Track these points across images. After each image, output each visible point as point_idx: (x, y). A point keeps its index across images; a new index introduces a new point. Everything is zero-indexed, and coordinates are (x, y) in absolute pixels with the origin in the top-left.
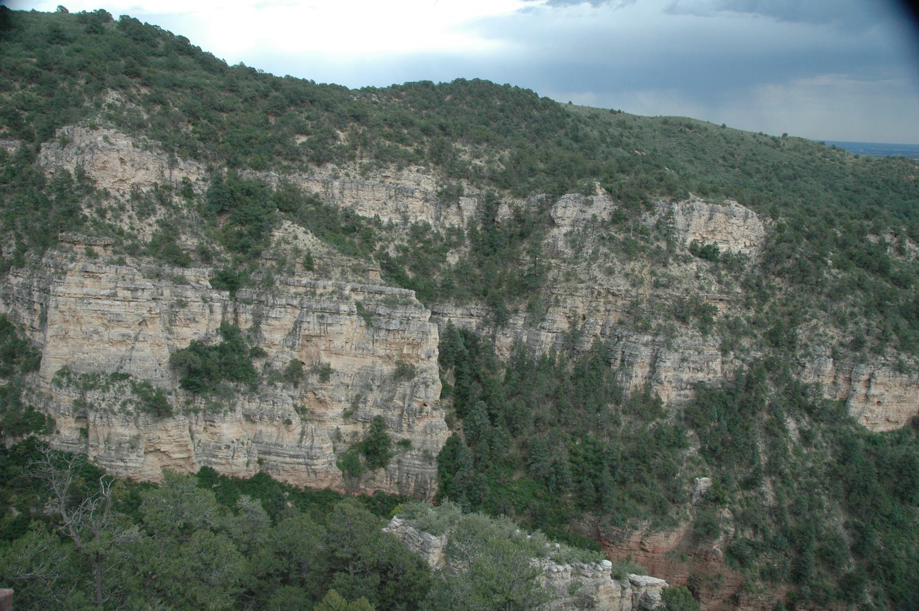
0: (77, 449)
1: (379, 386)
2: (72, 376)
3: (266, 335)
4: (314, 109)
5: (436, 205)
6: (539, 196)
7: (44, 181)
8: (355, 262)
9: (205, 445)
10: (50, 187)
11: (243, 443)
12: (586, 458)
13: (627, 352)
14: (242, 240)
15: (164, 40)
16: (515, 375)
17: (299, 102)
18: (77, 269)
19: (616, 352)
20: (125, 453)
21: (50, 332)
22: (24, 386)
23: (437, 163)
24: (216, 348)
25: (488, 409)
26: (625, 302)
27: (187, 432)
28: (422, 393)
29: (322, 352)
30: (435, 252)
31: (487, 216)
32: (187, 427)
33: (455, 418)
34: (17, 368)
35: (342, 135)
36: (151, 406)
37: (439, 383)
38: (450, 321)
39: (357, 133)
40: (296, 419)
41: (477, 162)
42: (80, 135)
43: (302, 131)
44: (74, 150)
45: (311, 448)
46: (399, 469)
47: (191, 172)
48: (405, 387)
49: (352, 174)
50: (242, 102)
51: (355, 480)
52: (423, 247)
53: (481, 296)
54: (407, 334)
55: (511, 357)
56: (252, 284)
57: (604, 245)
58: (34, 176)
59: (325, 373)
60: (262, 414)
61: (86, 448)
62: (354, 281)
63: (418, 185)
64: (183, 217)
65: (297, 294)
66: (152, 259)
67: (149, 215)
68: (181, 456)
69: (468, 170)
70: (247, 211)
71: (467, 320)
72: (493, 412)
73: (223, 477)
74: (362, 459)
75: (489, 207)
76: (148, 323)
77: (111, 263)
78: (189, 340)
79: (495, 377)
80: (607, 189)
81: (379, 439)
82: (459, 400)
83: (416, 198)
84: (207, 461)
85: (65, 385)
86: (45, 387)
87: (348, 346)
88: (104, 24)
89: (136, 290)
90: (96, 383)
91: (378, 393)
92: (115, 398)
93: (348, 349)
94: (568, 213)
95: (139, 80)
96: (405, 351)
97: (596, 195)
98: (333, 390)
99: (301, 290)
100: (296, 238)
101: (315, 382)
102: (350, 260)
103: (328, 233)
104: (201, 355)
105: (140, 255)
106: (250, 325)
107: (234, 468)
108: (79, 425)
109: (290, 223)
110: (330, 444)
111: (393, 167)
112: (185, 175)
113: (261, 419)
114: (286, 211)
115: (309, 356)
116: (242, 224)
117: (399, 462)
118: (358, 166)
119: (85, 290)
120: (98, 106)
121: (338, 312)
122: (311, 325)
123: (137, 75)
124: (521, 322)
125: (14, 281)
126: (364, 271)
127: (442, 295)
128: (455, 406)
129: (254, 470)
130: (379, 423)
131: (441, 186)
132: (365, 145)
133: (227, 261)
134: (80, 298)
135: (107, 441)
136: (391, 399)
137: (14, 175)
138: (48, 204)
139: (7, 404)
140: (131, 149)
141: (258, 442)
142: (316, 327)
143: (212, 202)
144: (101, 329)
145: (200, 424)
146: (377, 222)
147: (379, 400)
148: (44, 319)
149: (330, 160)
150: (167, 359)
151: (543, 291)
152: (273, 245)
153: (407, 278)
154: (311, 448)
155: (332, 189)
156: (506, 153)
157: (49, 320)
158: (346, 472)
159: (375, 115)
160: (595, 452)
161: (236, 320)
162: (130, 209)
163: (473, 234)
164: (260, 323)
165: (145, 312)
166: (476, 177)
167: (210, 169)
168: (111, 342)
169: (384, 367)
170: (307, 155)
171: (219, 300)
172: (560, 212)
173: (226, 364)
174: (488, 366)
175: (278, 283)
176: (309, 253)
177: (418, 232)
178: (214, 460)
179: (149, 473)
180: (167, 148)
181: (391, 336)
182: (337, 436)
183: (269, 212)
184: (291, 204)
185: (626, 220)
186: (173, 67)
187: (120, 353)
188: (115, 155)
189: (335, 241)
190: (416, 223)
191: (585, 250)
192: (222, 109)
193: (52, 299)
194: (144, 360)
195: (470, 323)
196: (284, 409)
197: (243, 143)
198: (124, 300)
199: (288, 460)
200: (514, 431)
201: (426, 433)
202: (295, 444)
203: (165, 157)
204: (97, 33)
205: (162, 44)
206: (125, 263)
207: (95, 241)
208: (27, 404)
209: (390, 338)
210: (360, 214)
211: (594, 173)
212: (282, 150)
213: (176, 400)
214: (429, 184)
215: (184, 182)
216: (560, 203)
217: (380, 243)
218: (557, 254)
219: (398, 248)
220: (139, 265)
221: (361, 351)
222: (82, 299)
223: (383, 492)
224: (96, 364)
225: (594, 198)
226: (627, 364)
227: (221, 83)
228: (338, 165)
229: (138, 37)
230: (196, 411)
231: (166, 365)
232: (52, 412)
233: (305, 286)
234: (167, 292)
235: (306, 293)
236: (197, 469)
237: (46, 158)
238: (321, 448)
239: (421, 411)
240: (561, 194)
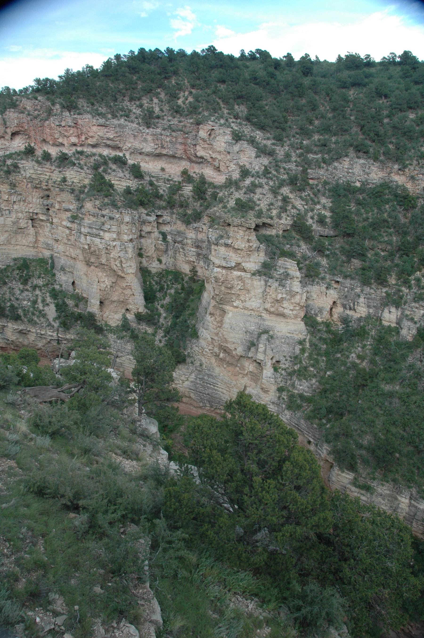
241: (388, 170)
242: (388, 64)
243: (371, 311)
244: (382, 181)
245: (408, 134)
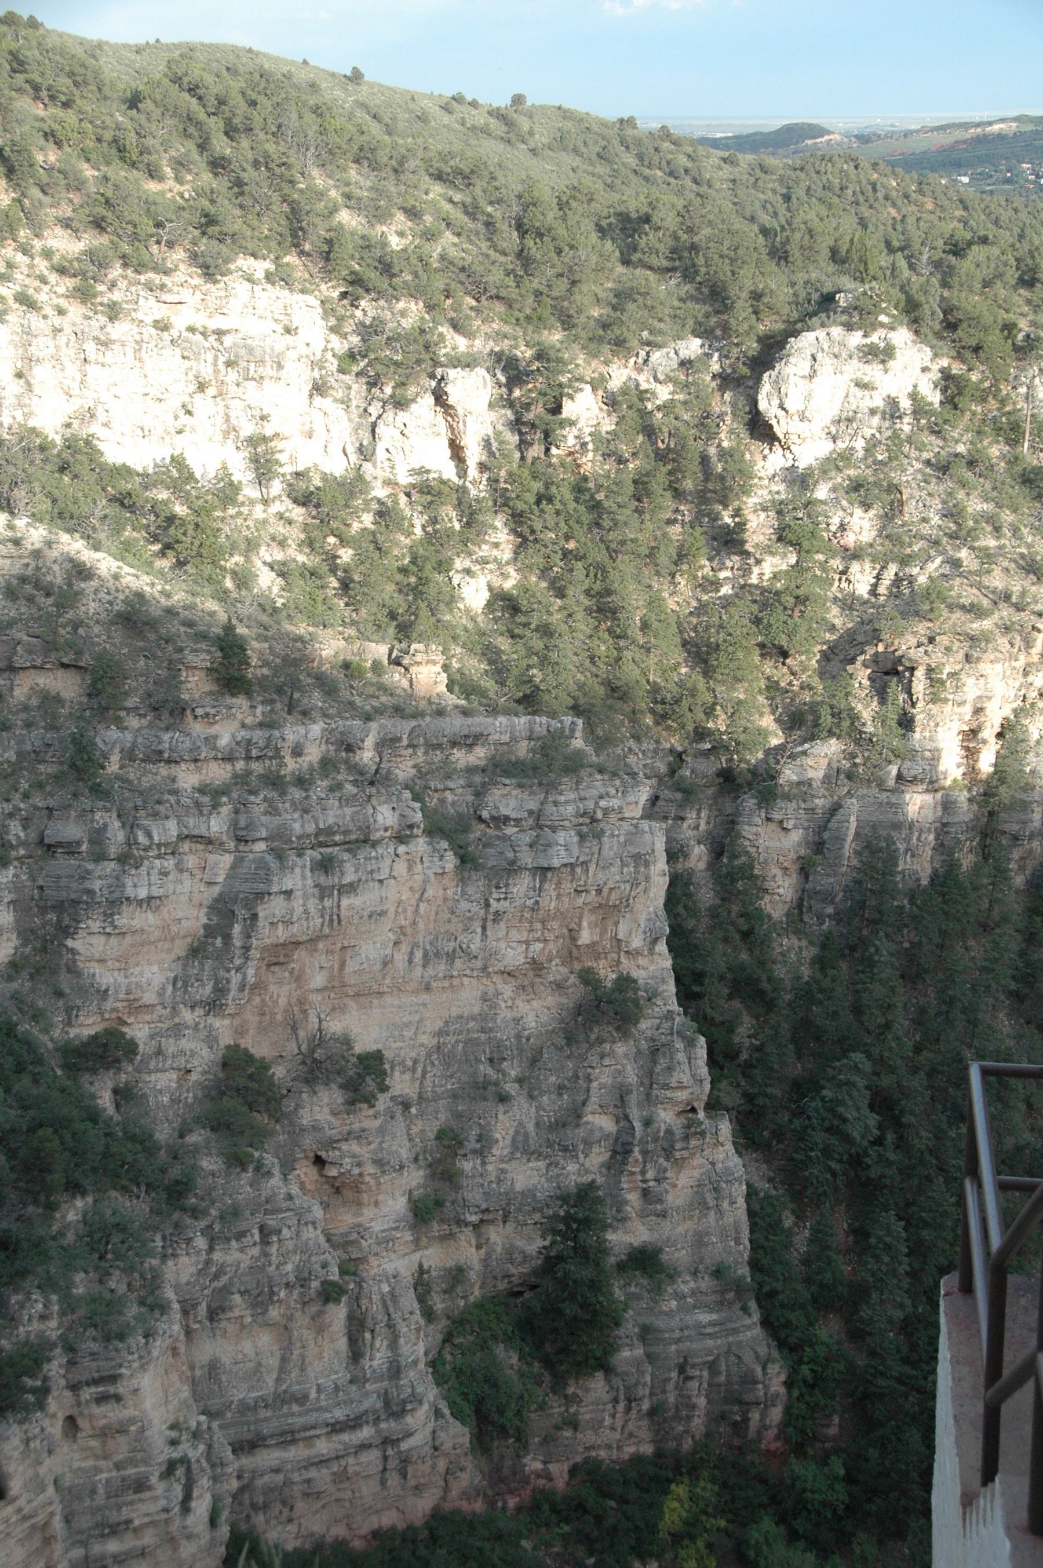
1: (520, 1081)
5: (345, 402)
45: (395, 1371)
46: (650, 1357)
54: (595, 875)
59: (362, 1076)
60: (225, 1291)
62: (379, 711)
75: (531, 399)
87: (400, 958)
96: (585, 937)
98: (381, 1131)
99: (218, 773)
117: (646, 1334)
118: (42, 265)
136: (576, 1113)
142: (313, 905)
147: (531, 1127)
169: (523, 1007)
196: (305, 1250)
202: (342, 1376)
221: (442, 968)
223: (598, 1463)
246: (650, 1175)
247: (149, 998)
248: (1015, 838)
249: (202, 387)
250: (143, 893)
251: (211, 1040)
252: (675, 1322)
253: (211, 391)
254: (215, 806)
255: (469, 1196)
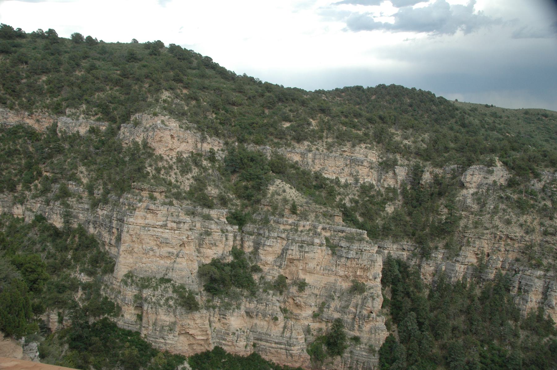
0: (134, 328)
1: (339, 297)
2: (134, 278)
3: (262, 257)
4: (295, 105)
5: (378, 171)
6: (452, 167)
7: (121, 148)
8: (325, 209)
9: (218, 331)
10: (125, 152)
11: (244, 332)
12: (493, 361)
13: (523, 282)
14: (248, 192)
15: (196, 59)
16: (437, 295)
17: (284, 100)
18: (143, 207)
19: (514, 282)
20: (166, 333)
21: (122, 248)
22: (102, 283)
23: (378, 143)
24: (228, 264)
25: (417, 318)
26: (520, 245)
27: (207, 322)
28: (369, 303)
29: (300, 271)
30: (377, 204)
31: (415, 179)
32: (208, 318)
33: (391, 323)
34: (99, 270)
35: (313, 122)
36: (185, 302)
37: (382, 297)
38: (389, 253)
39: (323, 121)
40: (281, 317)
41: (406, 142)
42: (146, 120)
43: (287, 119)
44: (142, 129)
45: (290, 338)
47: (214, 144)
48: (357, 299)
49: (321, 149)
50: (247, 100)
51: (319, 363)
52: (369, 200)
53: (411, 236)
54: (360, 261)
55: (433, 281)
56: (254, 222)
57: (502, 203)
58: (115, 145)
59: (302, 286)
60: (258, 312)
61: (140, 328)
62: (324, 223)
63: (366, 157)
64: (209, 175)
65: (285, 230)
66: (189, 202)
67: (187, 172)
68: (202, 338)
69: (400, 147)
70: (251, 172)
71: (401, 253)
72: (421, 320)
73: (229, 354)
74: (324, 348)
75: (416, 174)
76: (186, 245)
77: (164, 204)
78: (211, 258)
79: (421, 295)
80: (503, 162)
81: (338, 335)
82: (395, 310)
83: (364, 166)
84: (219, 342)
85: (130, 284)
86: (116, 284)
87: (318, 268)
88: (160, 49)
89: (179, 223)
90: (149, 284)
91: (338, 302)
92: (162, 295)
93: (318, 270)
94: (475, 179)
95: (182, 84)
96: (358, 273)
97: (496, 166)
98: (307, 298)
99: (288, 227)
100: (284, 191)
101: (294, 291)
102: (321, 208)
103: (305, 189)
104: (218, 268)
105: (182, 199)
106: (251, 250)
107: (237, 348)
108: (137, 312)
109: (280, 181)
110: (303, 336)
111: (349, 144)
112: (211, 147)
113: (257, 315)
114: (276, 173)
115: (291, 273)
116: (248, 181)
117: (351, 352)
118: (324, 143)
119: (147, 221)
120: (157, 100)
121: (313, 244)
122: (294, 252)
123: (181, 81)
124: (440, 256)
125: (100, 212)
126: (331, 216)
127: (383, 235)
128: (392, 314)
129: (250, 351)
130: (338, 323)
131: (381, 158)
132: (329, 129)
133: (237, 205)
134: (143, 227)
135: (155, 324)
136: (347, 307)
137: (103, 144)
138: (124, 163)
139: (91, 294)
140: (178, 129)
141: (253, 332)
142: (297, 253)
143: (228, 165)
144: (155, 248)
145: (216, 316)
146: (337, 182)
147: (338, 307)
148: (119, 239)
149: (306, 139)
150: (196, 270)
151: (456, 234)
152: (269, 195)
153: (358, 221)
154: (290, 338)
155: (307, 158)
156: (426, 136)
157: (122, 240)
158: (313, 356)
159: (335, 109)
160: (500, 356)
161: (242, 246)
162: (176, 168)
163: (404, 192)
164: (258, 248)
165: (184, 238)
166: (406, 152)
167: (226, 143)
168: (161, 257)
170: (290, 136)
171: (231, 232)
172: (468, 178)
173: (235, 276)
174: (416, 286)
175: (272, 222)
176: (294, 202)
177: (365, 189)
178: (224, 342)
179: (180, 348)
180: (199, 129)
181: (349, 262)
182: (308, 331)
183: (266, 173)
184: (280, 168)
185: (519, 184)
186: (203, 76)
187: (166, 265)
188: (168, 133)
189: (309, 194)
190: (364, 183)
191: (487, 206)
192: (234, 104)
193: (126, 226)
194: (181, 270)
195: (402, 255)
196: (273, 310)
197: (248, 127)
198: (172, 229)
199: (273, 345)
200: (437, 336)
201: (372, 333)
202: (279, 334)
203: (199, 134)
204: (156, 55)
205: (195, 62)
206: (173, 205)
207: (155, 189)
208: (104, 295)
209: (349, 263)
210: (326, 176)
211: (493, 150)
212: (274, 131)
213: (201, 299)
214: (373, 156)
215: (210, 152)
216: (469, 172)
217: (339, 197)
218: (466, 208)
219: (351, 200)
220: (181, 206)
221: (327, 272)
222: (144, 227)
224: (150, 271)
225: (495, 169)
226: (523, 291)
227: (233, 87)
228: (311, 142)
229: (181, 57)
230: (214, 307)
231: (195, 274)
232: (119, 302)
233: (291, 225)
234: (198, 225)
235: (291, 230)
236: (212, 348)
237: (124, 134)
238: (297, 339)
239: (369, 317)
240: (469, 166)
241: (22, 116)
242: (38, 36)
243: (6, 210)
244: (18, 123)
245: (40, 92)
246: (361, 323)
247: (269, 263)
248: (484, 280)
249: (347, 165)
250: (268, 244)
251: (279, 272)
252: (357, 352)
253: (349, 166)
254: (284, 232)
255: (324, 315)
